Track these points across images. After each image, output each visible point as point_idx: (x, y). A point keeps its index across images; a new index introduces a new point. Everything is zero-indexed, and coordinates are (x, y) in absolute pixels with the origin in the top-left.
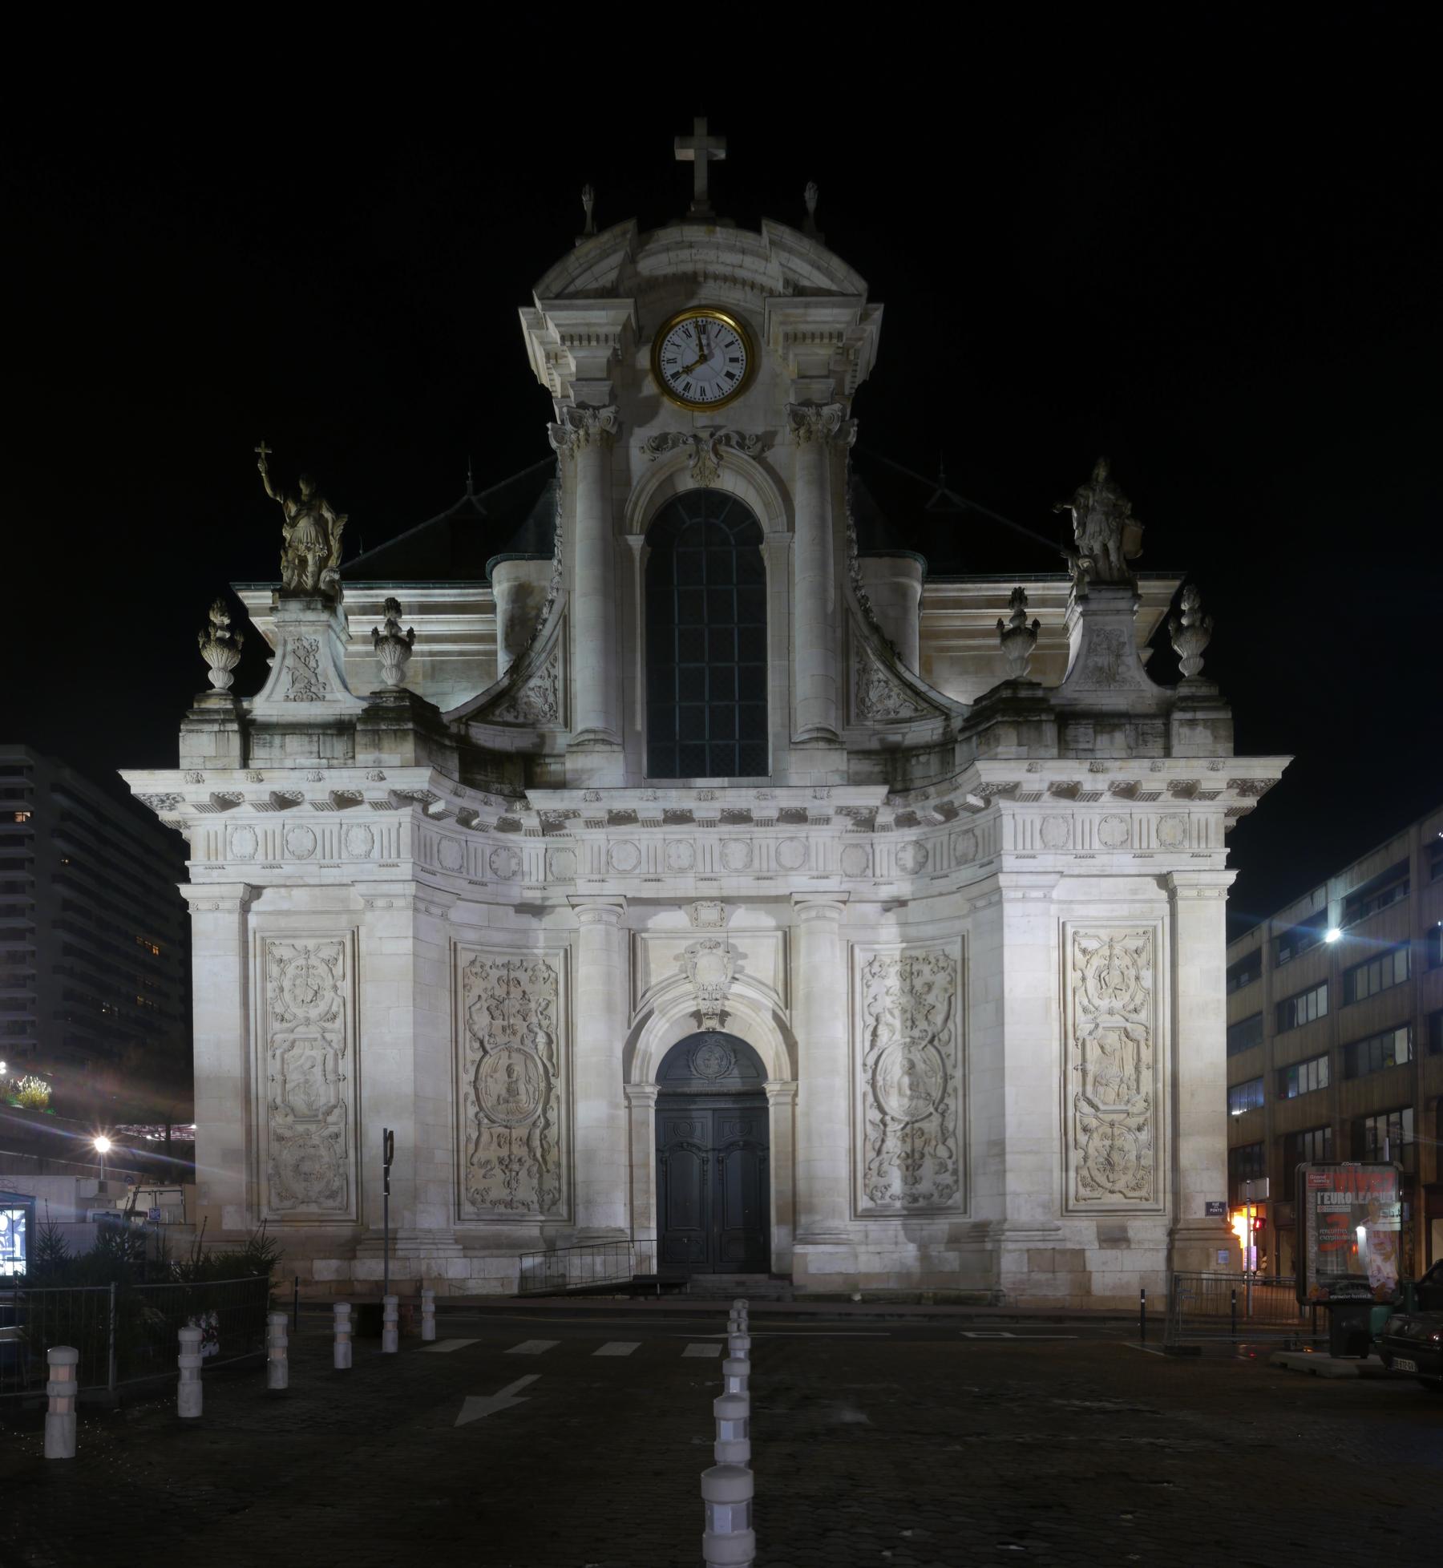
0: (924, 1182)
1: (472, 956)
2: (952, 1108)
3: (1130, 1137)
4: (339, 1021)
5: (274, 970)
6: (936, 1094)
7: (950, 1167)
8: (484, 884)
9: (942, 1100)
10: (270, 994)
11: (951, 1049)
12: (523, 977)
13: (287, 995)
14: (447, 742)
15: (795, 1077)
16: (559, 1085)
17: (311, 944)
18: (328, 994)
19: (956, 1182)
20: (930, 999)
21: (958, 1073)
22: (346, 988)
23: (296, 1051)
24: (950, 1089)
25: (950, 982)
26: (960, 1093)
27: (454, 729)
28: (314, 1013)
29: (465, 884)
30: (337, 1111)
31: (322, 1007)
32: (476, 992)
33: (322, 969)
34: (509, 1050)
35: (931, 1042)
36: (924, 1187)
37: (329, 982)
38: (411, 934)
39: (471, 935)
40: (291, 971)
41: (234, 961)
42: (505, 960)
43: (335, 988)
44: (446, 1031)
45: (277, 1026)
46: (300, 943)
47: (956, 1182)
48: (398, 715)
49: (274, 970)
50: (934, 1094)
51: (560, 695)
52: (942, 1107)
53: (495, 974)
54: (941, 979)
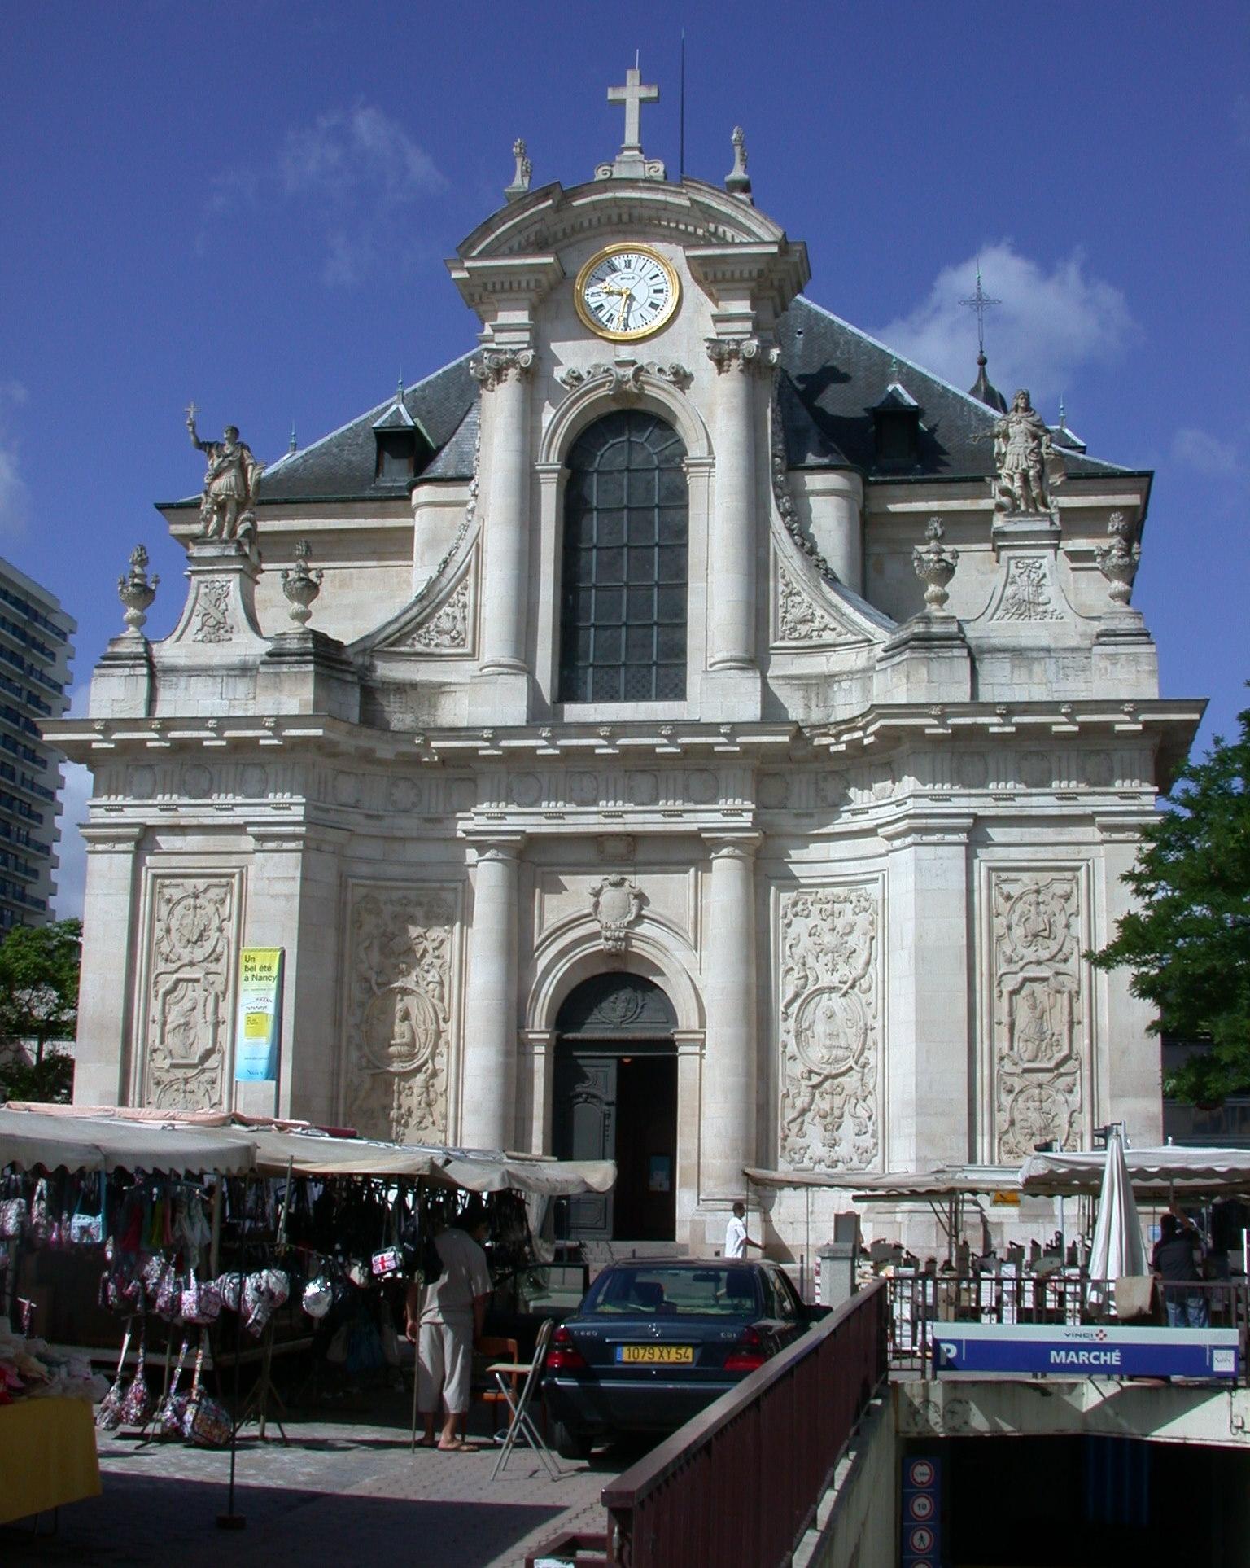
0: (843, 1143)
1: (363, 891)
2: (872, 1062)
5: (164, 909)
6: (856, 1046)
7: (870, 1128)
8: (379, 818)
9: (862, 1053)
10: (158, 933)
11: (871, 996)
13: (174, 935)
15: (702, 1024)
16: (451, 1028)
17: (201, 883)
19: (876, 1144)
21: (878, 1024)
22: (231, 928)
23: (179, 992)
24: (870, 1042)
28: (199, 954)
29: (360, 819)
30: (215, 1058)
31: (208, 946)
33: (211, 908)
35: (852, 987)
36: (843, 1150)
37: (215, 923)
39: (364, 869)
40: (179, 910)
41: (125, 900)
42: (396, 895)
45: (162, 966)
46: (189, 883)
47: (876, 1144)
49: (164, 909)
50: (854, 1046)
52: (862, 1060)
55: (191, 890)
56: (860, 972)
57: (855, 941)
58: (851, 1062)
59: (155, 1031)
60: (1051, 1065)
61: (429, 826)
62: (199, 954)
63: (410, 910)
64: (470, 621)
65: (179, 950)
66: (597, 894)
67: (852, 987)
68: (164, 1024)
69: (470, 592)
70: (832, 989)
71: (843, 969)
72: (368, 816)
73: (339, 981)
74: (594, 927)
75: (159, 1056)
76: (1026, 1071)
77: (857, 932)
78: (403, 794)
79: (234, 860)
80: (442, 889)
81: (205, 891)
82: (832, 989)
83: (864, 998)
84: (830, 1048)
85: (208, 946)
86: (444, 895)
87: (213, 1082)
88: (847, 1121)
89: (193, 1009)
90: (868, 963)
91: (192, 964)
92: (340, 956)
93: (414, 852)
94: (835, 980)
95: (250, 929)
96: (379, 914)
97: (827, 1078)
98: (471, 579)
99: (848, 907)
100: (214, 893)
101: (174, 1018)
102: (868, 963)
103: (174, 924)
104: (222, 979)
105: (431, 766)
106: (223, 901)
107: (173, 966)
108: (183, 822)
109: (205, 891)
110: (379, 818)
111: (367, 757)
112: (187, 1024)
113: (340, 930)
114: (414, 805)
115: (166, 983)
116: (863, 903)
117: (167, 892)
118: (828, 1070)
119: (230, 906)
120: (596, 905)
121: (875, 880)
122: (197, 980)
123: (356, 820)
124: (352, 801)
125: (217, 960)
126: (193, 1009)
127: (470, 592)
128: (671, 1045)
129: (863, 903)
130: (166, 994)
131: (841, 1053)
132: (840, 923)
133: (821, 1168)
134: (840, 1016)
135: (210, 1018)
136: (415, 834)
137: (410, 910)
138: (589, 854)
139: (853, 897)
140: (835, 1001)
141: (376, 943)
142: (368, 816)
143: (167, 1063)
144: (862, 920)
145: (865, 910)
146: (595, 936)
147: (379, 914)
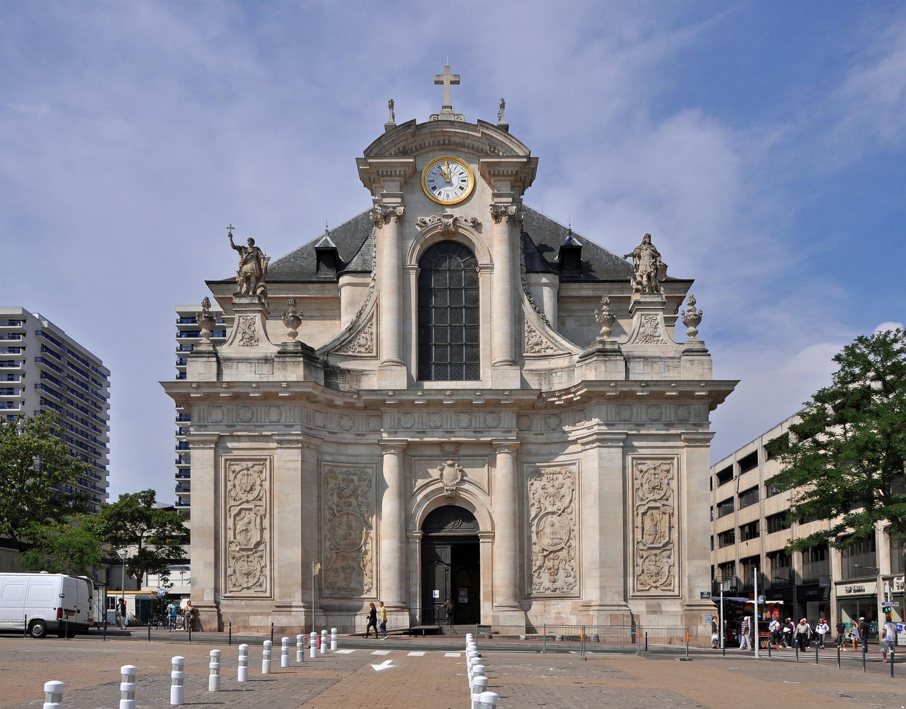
1: (329, 468)
2: (573, 545)
3: (665, 560)
4: (263, 503)
5: (232, 476)
6: (565, 538)
7: (572, 574)
8: (335, 433)
9: (568, 541)
10: (229, 487)
12: (355, 478)
13: (238, 488)
14: (318, 365)
15: (493, 528)
17: (250, 464)
18: (258, 488)
20: (563, 491)
21: (576, 528)
23: (242, 515)
24: (572, 536)
25: (573, 483)
26: (577, 538)
27: (321, 358)
28: (251, 497)
29: (326, 433)
32: (331, 485)
34: (348, 514)
35: (563, 512)
37: (259, 482)
38: (300, 458)
39: (328, 458)
40: (239, 476)
42: (346, 469)
43: (261, 485)
44: (315, 505)
45: (232, 503)
48: (295, 354)
49: (232, 476)
50: (564, 538)
51: (375, 341)
53: (340, 477)
54: (568, 482)
55: (245, 467)
56: (566, 504)
58: (563, 545)
62: (251, 497)
63: (351, 477)
65: (240, 495)
66: (442, 470)
67: (563, 512)
68: (235, 530)
70: (553, 513)
71: (558, 504)
72: (330, 432)
73: (319, 509)
74: (440, 485)
75: (233, 546)
78: (346, 422)
79: (266, 452)
81: (252, 467)
82: (553, 513)
83: (569, 517)
84: (553, 539)
85: (255, 493)
86: (367, 470)
87: (261, 557)
88: (561, 571)
89: (249, 523)
90: (571, 501)
91: (247, 502)
92: (319, 497)
93: (351, 450)
95: (276, 485)
96: (336, 479)
97: (551, 552)
99: (560, 476)
100: (256, 468)
101: (240, 526)
102: (571, 501)
103: (237, 482)
105: (359, 409)
106: (261, 472)
107: (237, 503)
109: (252, 467)
110: (335, 433)
111: (330, 404)
112: (247, 530)
113: (319, 486)
114: (351, 428)
115: (235, 511)
116: (568, 474)
117: (233, 468)
118: (551, 549)
119: (266, 474)
120: (441, 475)
122: (250, 509)
123: (324, 434)
124: (322, 425)
125: (260, 500)
126: (249, 523)
128: (476, 539)
129: (568, 474)
130: (235, 516)
131: (558, 541)
133: (548, 593)
135: (258, 526)
136: (352, 441)
137: (351, 477)
138: (436, 451)
139: (563, 471)
140: (555, 518)
141: (335, 492)
142: (330, 432)
143: (238, 549)
144: (568, 482)
146: (442, 489)
147: (336, 479)
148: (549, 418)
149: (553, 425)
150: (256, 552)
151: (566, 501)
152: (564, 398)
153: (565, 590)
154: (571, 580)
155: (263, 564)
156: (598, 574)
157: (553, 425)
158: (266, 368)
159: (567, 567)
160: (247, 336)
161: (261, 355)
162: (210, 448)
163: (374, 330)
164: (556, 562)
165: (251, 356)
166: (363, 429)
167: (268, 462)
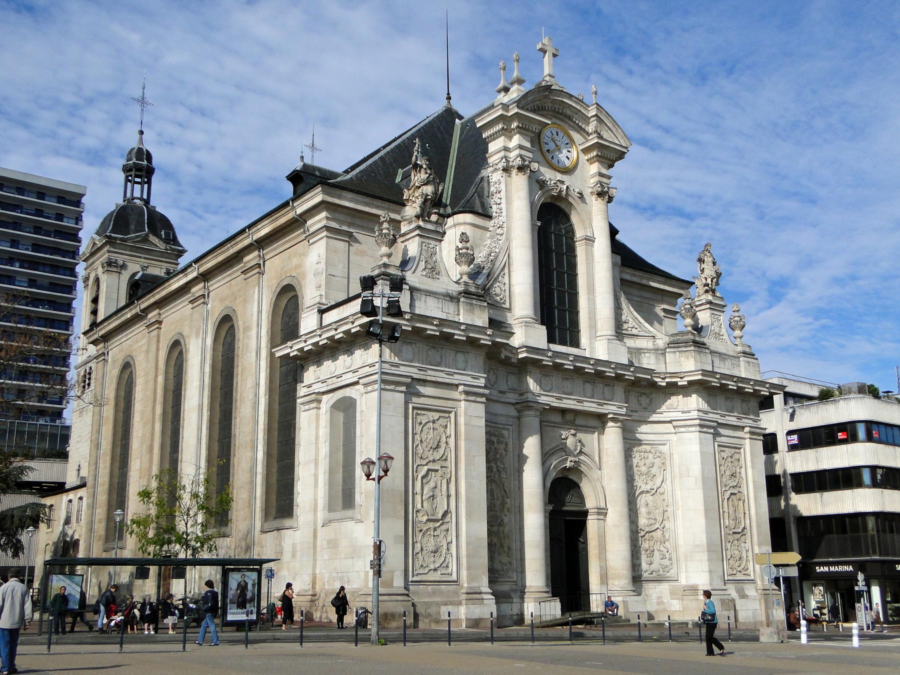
5: (418, 428)
10: (416, 443)
13: (424, 445)
17: (436, 415)
37: (444, 439)
55: (431, 419)
56: (659, 483)
57: (653, 470)
58: (658, 525)
59: (418, 498)
60: (740, 530)
61: (500, 395)
64: (507, 291)
69: (506, 277)
70: (648, 492)
75: (420, 515)
76: (734, 533)
77: (655, 467)
79: (450, 404)
80: (504, 429)
81: (438, 420)
82: (648, 492)
83: (661, 497)
84: (649, 519)
88: (656, 553)
89: (436, 487)
91: (434, 461)
94: (648, 487)
98: (506, 270)
99: (651, 456)
100: (441, 421)
103: (424, 437)
104: (449, 470)
107: (424, 462)
108: (429, 378)
109: (438, 420)
112: (433, 496)
116: (658, 454)
117: (419, 418)
118: (647, 529)
121: (664, 444)
122: (437, 471)
126: (436, 487)
127: (506, 277)
130: (423, 478)
131: (653, 521)
132: (648, 462)
134: (650, 503)
139: (653, 451)
143: (425, 518)
144: (658, 461)
145: (659, 457)
148: (641, 396)
149: (644, 404)
150: (442, 524)
151: (658, 481)
152: (667, 380)
153: (661, 572)
154: (666, 562)
155: (449, 540)
156: (706, 558)
157: (644, 404)
158: (451, 308)
159: (662, 548)
160: (429, 266)
161: (443, 291)
162: (401, 392)
163: (506, 280)
164: (652, 543)
165: (434, 289)
166: (504, 387)
167: (452, 415)
